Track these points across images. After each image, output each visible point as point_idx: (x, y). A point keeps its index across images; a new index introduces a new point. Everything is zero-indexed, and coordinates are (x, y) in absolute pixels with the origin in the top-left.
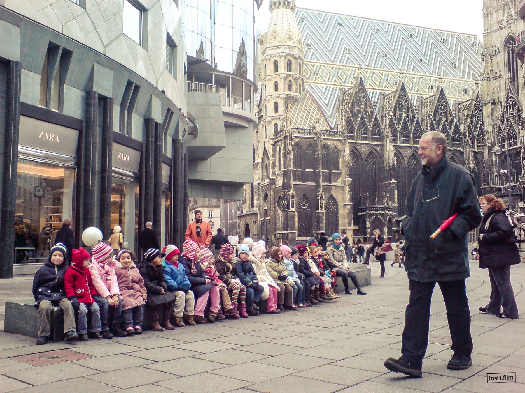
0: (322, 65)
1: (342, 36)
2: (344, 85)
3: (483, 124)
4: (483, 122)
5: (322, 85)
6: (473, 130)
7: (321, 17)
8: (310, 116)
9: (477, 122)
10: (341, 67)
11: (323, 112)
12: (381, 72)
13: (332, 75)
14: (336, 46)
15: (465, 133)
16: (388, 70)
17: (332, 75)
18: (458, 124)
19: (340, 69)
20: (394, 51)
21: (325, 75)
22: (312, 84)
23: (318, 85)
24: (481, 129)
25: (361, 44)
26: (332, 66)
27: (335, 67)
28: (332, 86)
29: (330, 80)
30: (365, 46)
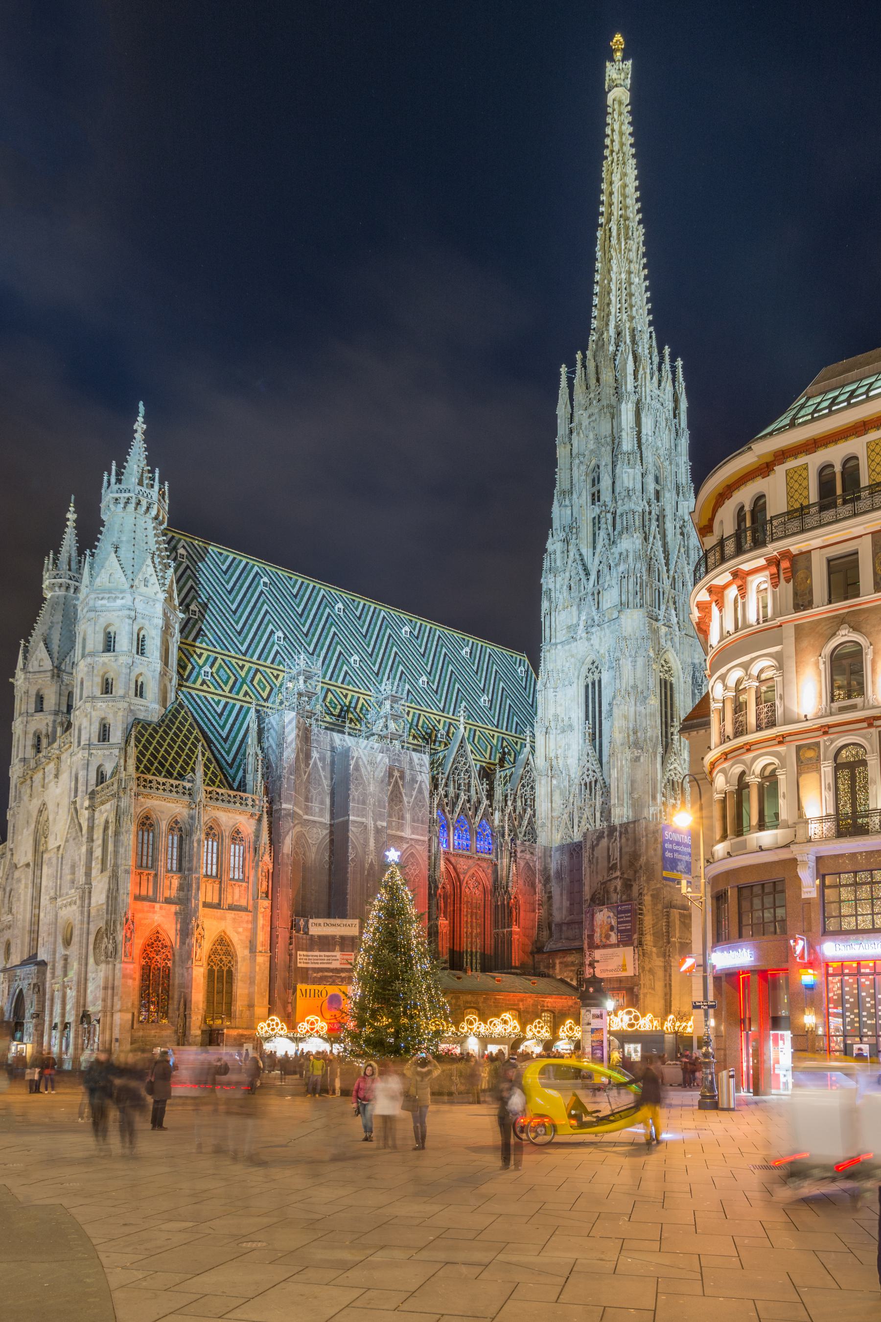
0: (219, 656)
1: (265, 607)
2: (264, 704)
3: (534, 816)
4: (534, 812)
5: (216, 698)
6: (516, 823)
7: (225, 560)
8: (184, 757)
9: (525, 811)
10: (261, 668)
11: (216, 752)
12: (345, 692)
13: (240, 680)
14: (252, 625)
15: (503, 827)
16: (357, 690)
17: (240, 680)
18: (490, 810)
19: (257, 670)
20: (371, 655)
21: (224, 678)
22: (193, 692)
23: (209, 696)
24: (530, 823)
25: (305, 630)
26: (241, 663)
27: (247, 665)
28: (238, 704)
29: (236, 689)
30: (313, 635)
